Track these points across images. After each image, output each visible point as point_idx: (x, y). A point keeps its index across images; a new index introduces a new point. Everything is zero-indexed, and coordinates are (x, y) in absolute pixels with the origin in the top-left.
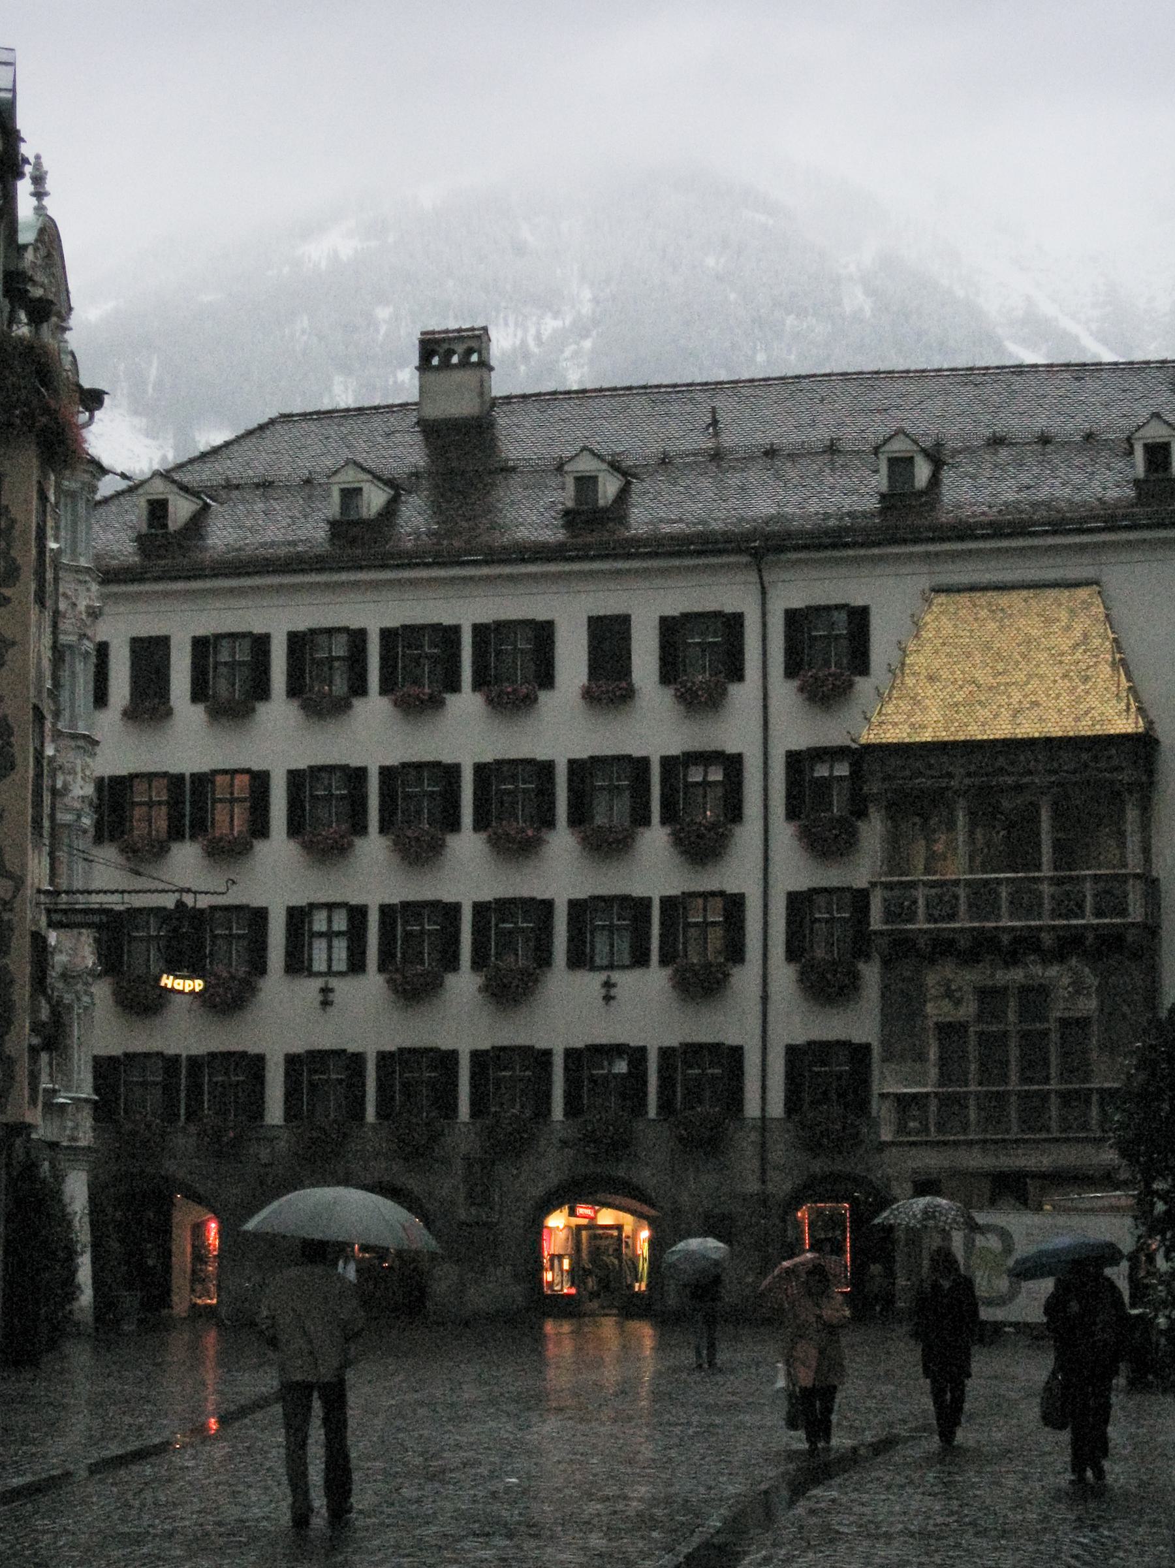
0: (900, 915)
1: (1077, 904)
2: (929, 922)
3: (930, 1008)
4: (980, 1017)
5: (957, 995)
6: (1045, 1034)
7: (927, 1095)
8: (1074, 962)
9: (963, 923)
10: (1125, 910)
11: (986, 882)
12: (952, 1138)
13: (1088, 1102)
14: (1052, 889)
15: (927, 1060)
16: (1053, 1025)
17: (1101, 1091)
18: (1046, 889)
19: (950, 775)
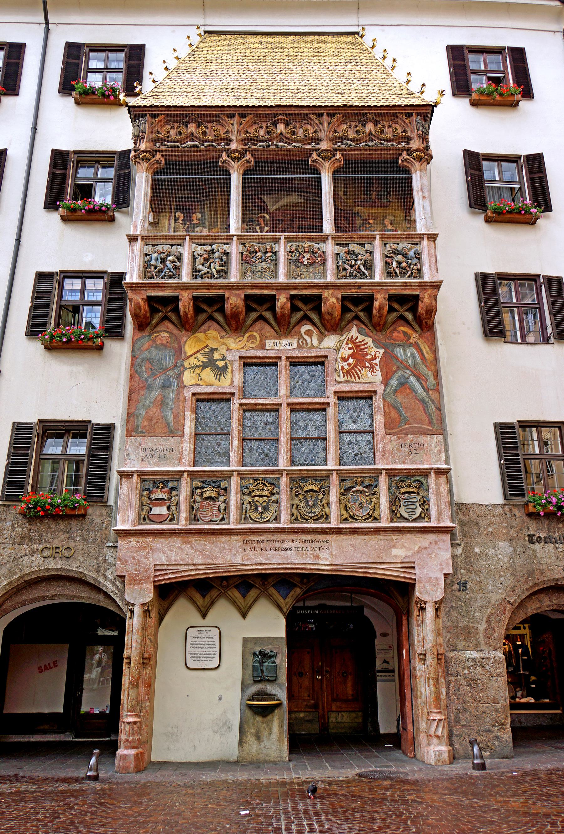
0: (161, 271)
1: (365, 266)
2: (196, 277)
3: (188, 378)
4: (244, 393)
5: (221, 364)
6: (322, 408)
7: (181, 473)
8: (354, 332)
9: (234, 278)
10: (419, 270)
11: (261, 240)
12: (206, 527)
13: (373, 486)
14: (338, 249)
15: (182, 436)
16: (332, 400)
17: (391, 473)
18: (330, 248)
19: (228, 141)
